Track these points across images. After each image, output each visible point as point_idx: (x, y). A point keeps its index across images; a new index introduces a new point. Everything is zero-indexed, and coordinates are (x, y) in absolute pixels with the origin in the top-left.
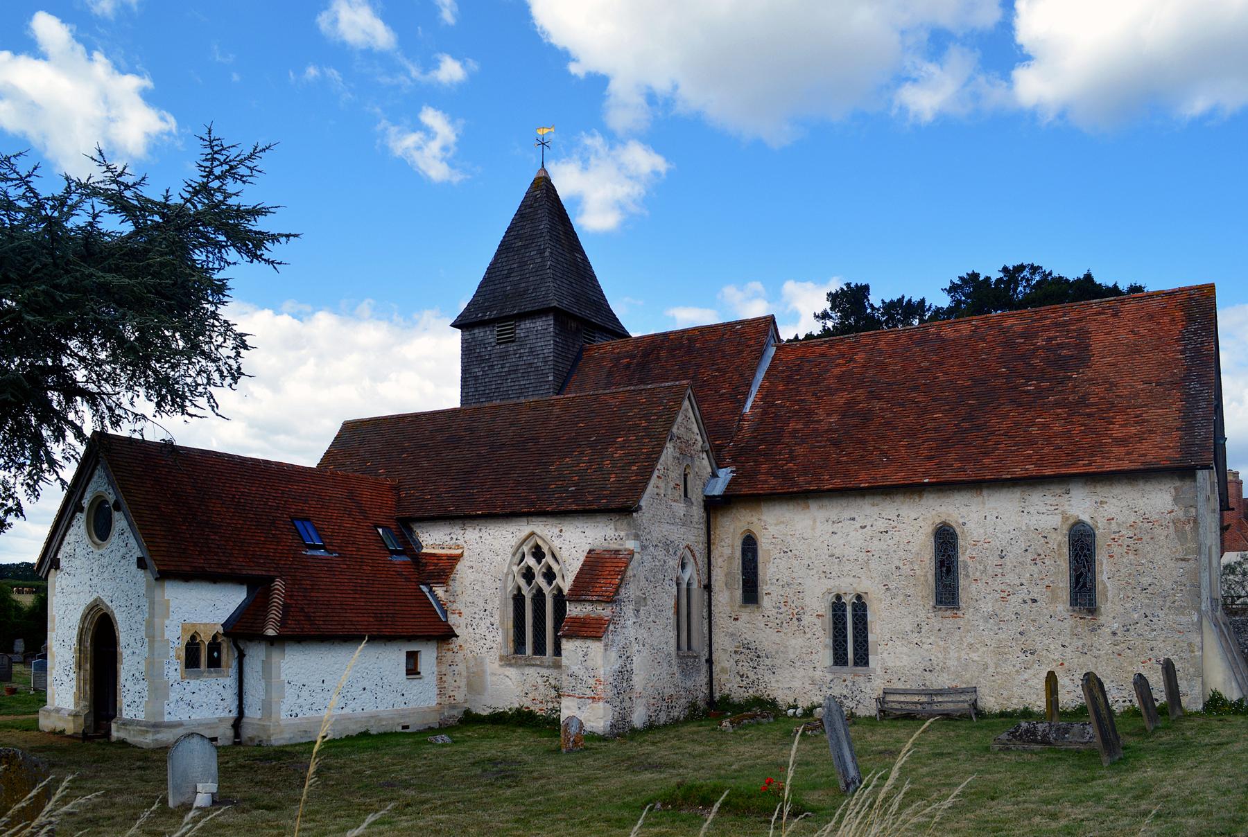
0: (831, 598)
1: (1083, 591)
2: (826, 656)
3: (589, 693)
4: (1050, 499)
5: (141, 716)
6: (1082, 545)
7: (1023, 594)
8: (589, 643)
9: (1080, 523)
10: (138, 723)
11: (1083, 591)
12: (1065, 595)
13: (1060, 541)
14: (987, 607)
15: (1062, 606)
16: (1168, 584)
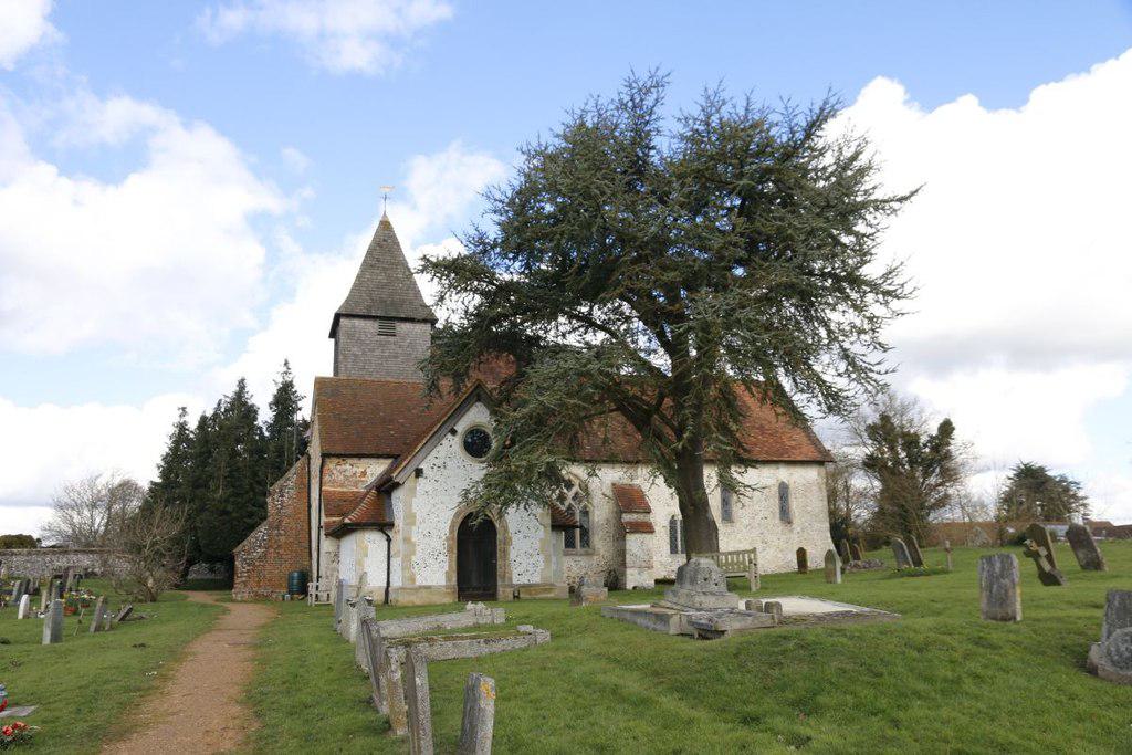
0: (670, 517)
1: (785, 515)
2: (667, 548)
3: (644, 564)
4: (772, 471)
5: (536, 579)
6: (784, 491)
7: (761, 515)
8: (645, 535)
9: (783, 482)
10: (535, 585)
11: (785, 515)
12: (778, 516)
13: (775, 489)
14: (746, 521)
15: (777, 521)
16: (817, 510)
